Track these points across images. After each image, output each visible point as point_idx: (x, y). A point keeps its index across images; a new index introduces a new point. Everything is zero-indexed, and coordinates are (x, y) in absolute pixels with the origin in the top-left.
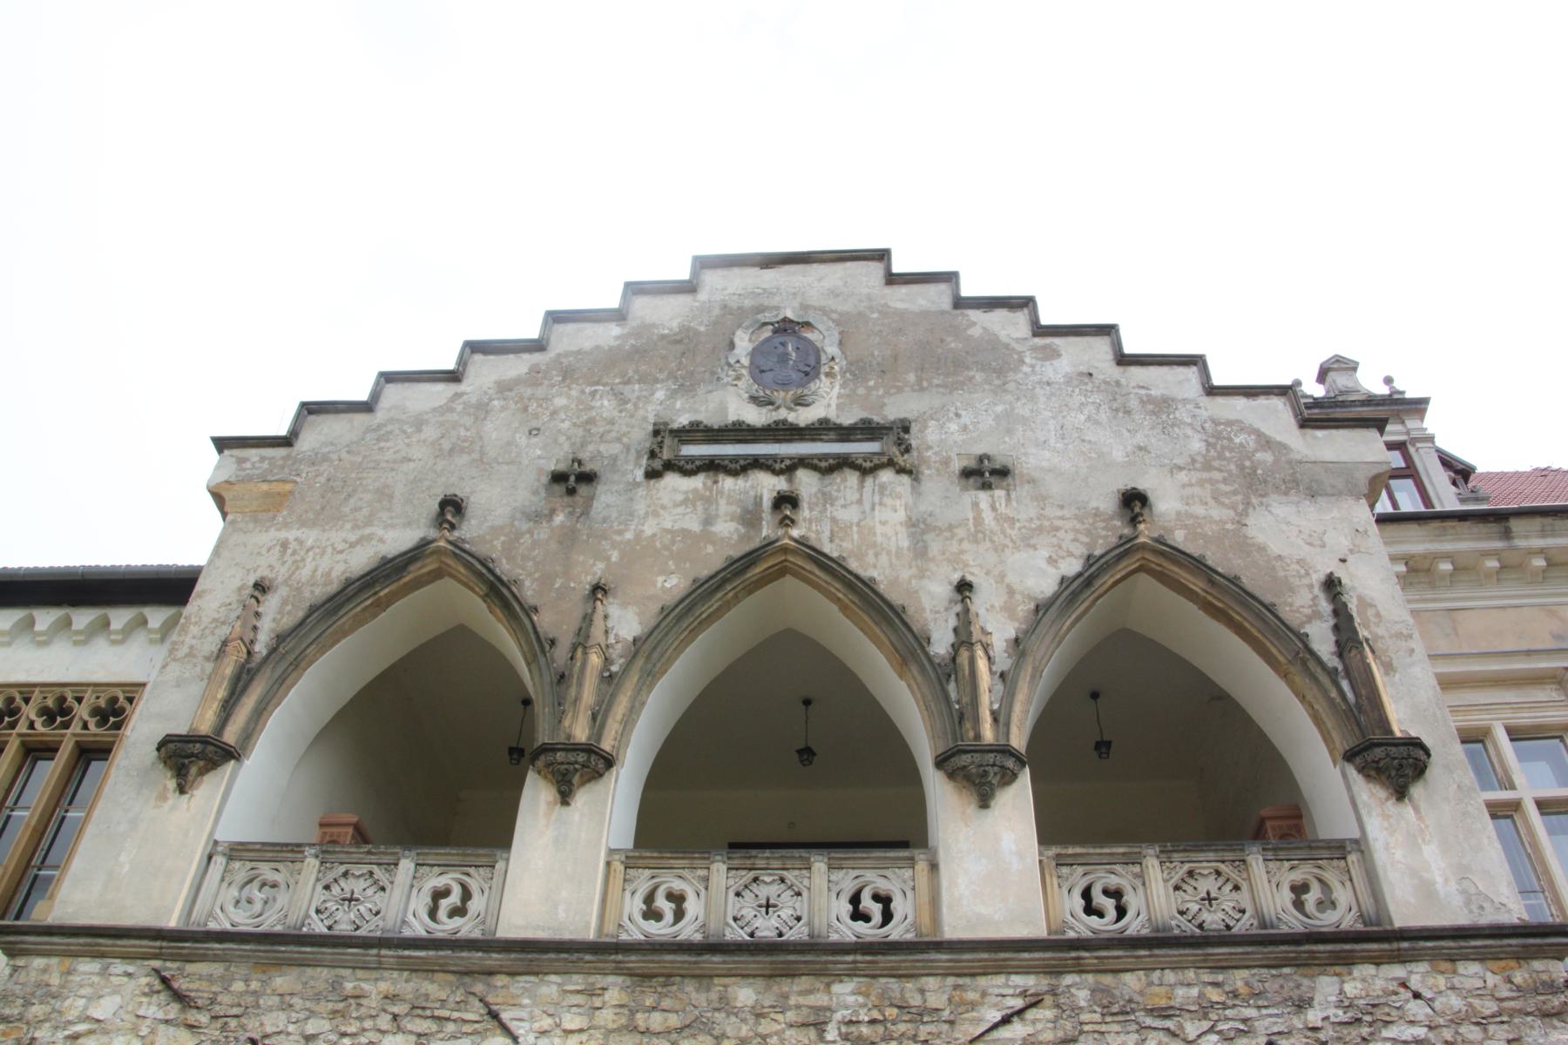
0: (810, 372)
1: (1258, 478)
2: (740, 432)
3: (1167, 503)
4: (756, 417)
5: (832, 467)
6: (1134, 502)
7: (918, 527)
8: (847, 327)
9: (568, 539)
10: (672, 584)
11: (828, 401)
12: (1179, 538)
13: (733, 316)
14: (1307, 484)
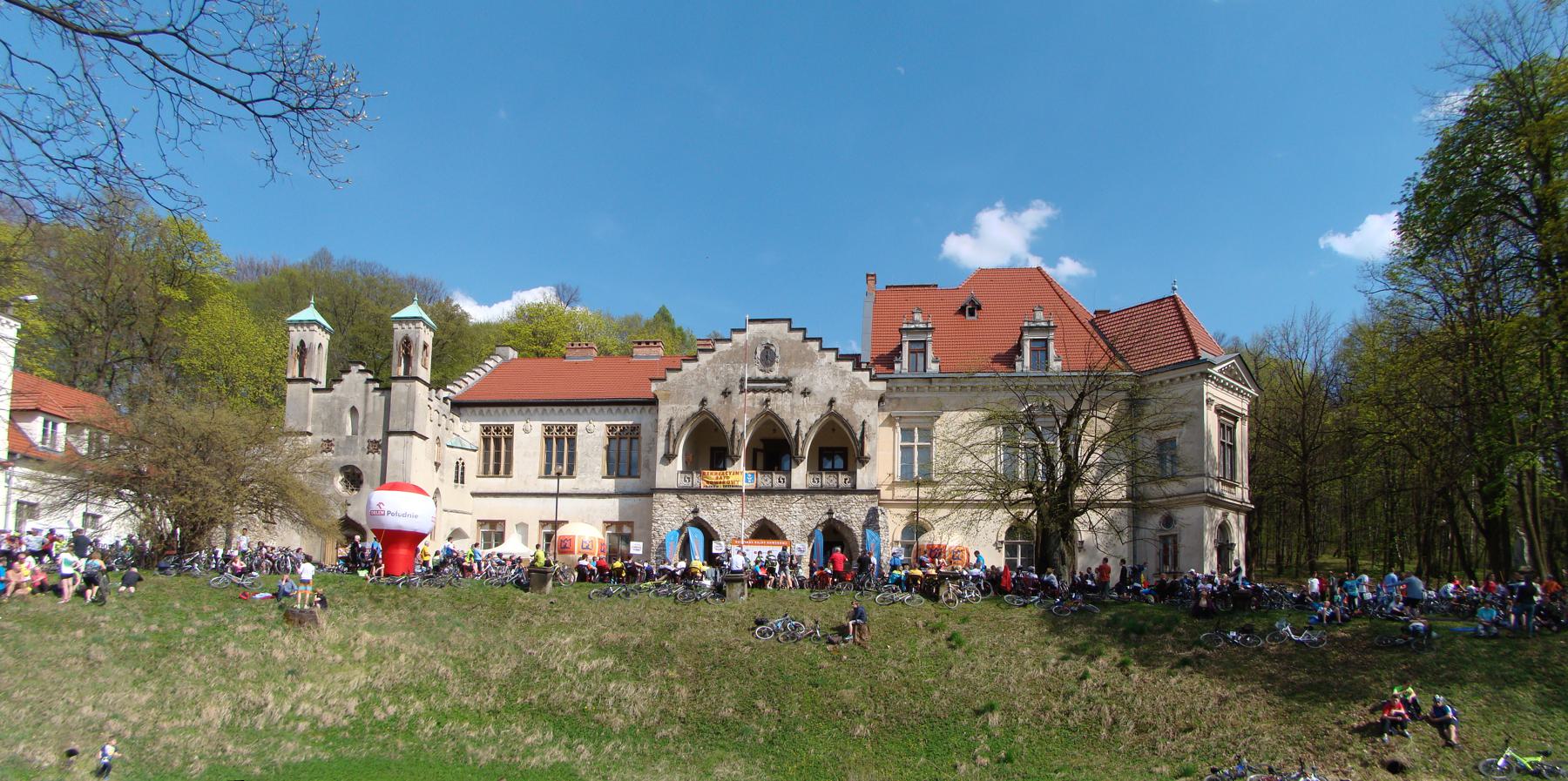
0: (773, 362)
1: (858, 394)
2: (758, 380)
3: (839, 402)
4: (761, 375)
5: (779, 390)
6: (832, 402)
7: (792, 406)
8: (781, 343)
9: (728, 409)
10: (746, 419)
11: (776, 371)
12: (840, 411)
13: (757, 340)
14: (867, 396)
